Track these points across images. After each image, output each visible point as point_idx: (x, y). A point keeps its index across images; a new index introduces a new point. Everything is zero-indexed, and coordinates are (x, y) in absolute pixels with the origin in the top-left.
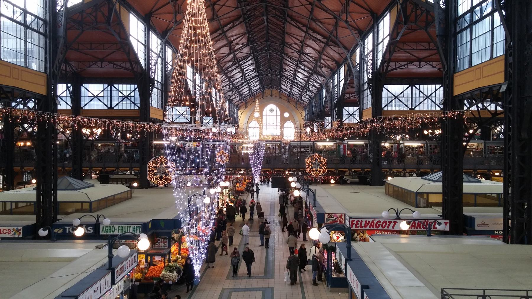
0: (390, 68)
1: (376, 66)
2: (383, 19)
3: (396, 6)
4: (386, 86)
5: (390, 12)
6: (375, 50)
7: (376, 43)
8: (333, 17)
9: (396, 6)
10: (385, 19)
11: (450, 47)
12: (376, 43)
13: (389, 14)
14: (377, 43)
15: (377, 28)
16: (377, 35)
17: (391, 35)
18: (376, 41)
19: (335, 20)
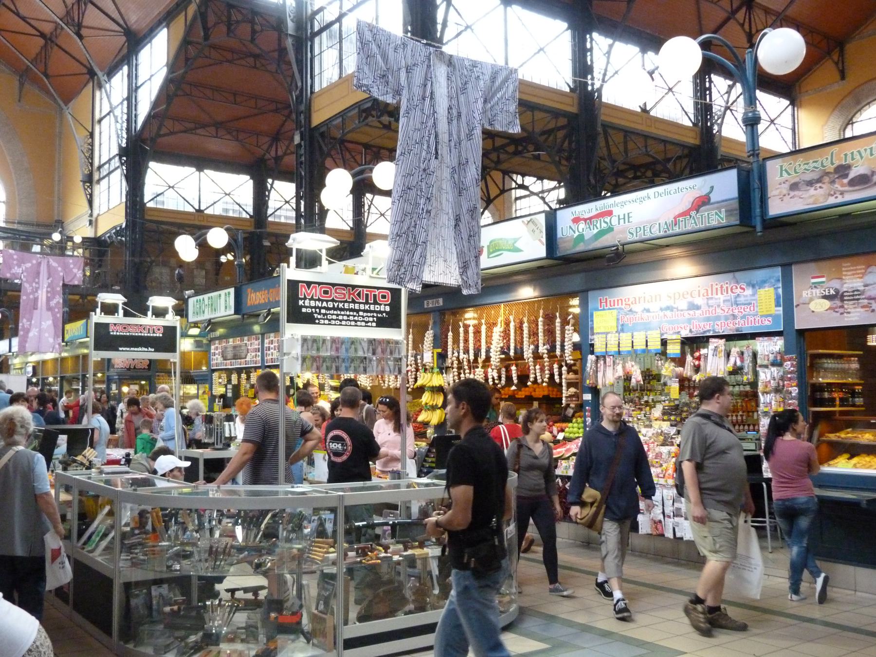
0: (164, 131)
1: (133, 125)
2: (150, 41)
3: (184, 13)
4: (152, 165)
5: (168, 26)
6: (131, 100)
7: (134, 85)
8: (39, 34)
9: (184, 13)
10: (154, 41)
11: (306, 54)
12: (134, 85)
13: (164, 32)
14: (136, 86)
15: (136, 60)
16: (136, 70)
17: (172, 66)
18: (134, 81)
19: (41, 42)
